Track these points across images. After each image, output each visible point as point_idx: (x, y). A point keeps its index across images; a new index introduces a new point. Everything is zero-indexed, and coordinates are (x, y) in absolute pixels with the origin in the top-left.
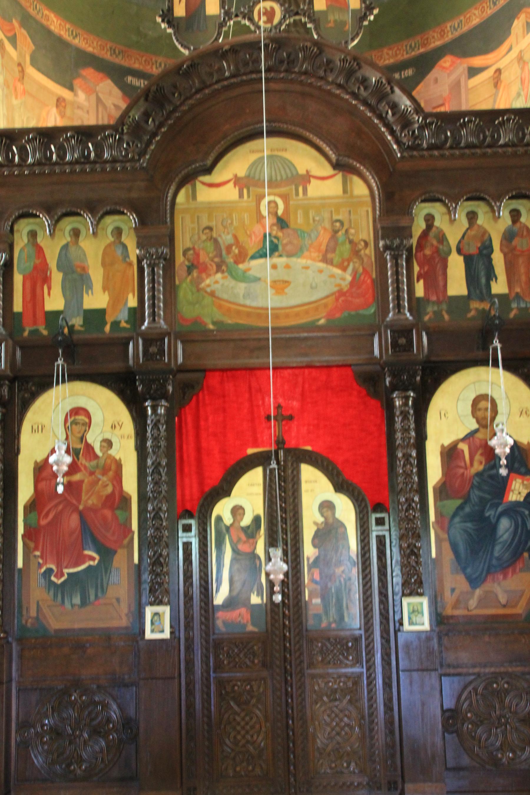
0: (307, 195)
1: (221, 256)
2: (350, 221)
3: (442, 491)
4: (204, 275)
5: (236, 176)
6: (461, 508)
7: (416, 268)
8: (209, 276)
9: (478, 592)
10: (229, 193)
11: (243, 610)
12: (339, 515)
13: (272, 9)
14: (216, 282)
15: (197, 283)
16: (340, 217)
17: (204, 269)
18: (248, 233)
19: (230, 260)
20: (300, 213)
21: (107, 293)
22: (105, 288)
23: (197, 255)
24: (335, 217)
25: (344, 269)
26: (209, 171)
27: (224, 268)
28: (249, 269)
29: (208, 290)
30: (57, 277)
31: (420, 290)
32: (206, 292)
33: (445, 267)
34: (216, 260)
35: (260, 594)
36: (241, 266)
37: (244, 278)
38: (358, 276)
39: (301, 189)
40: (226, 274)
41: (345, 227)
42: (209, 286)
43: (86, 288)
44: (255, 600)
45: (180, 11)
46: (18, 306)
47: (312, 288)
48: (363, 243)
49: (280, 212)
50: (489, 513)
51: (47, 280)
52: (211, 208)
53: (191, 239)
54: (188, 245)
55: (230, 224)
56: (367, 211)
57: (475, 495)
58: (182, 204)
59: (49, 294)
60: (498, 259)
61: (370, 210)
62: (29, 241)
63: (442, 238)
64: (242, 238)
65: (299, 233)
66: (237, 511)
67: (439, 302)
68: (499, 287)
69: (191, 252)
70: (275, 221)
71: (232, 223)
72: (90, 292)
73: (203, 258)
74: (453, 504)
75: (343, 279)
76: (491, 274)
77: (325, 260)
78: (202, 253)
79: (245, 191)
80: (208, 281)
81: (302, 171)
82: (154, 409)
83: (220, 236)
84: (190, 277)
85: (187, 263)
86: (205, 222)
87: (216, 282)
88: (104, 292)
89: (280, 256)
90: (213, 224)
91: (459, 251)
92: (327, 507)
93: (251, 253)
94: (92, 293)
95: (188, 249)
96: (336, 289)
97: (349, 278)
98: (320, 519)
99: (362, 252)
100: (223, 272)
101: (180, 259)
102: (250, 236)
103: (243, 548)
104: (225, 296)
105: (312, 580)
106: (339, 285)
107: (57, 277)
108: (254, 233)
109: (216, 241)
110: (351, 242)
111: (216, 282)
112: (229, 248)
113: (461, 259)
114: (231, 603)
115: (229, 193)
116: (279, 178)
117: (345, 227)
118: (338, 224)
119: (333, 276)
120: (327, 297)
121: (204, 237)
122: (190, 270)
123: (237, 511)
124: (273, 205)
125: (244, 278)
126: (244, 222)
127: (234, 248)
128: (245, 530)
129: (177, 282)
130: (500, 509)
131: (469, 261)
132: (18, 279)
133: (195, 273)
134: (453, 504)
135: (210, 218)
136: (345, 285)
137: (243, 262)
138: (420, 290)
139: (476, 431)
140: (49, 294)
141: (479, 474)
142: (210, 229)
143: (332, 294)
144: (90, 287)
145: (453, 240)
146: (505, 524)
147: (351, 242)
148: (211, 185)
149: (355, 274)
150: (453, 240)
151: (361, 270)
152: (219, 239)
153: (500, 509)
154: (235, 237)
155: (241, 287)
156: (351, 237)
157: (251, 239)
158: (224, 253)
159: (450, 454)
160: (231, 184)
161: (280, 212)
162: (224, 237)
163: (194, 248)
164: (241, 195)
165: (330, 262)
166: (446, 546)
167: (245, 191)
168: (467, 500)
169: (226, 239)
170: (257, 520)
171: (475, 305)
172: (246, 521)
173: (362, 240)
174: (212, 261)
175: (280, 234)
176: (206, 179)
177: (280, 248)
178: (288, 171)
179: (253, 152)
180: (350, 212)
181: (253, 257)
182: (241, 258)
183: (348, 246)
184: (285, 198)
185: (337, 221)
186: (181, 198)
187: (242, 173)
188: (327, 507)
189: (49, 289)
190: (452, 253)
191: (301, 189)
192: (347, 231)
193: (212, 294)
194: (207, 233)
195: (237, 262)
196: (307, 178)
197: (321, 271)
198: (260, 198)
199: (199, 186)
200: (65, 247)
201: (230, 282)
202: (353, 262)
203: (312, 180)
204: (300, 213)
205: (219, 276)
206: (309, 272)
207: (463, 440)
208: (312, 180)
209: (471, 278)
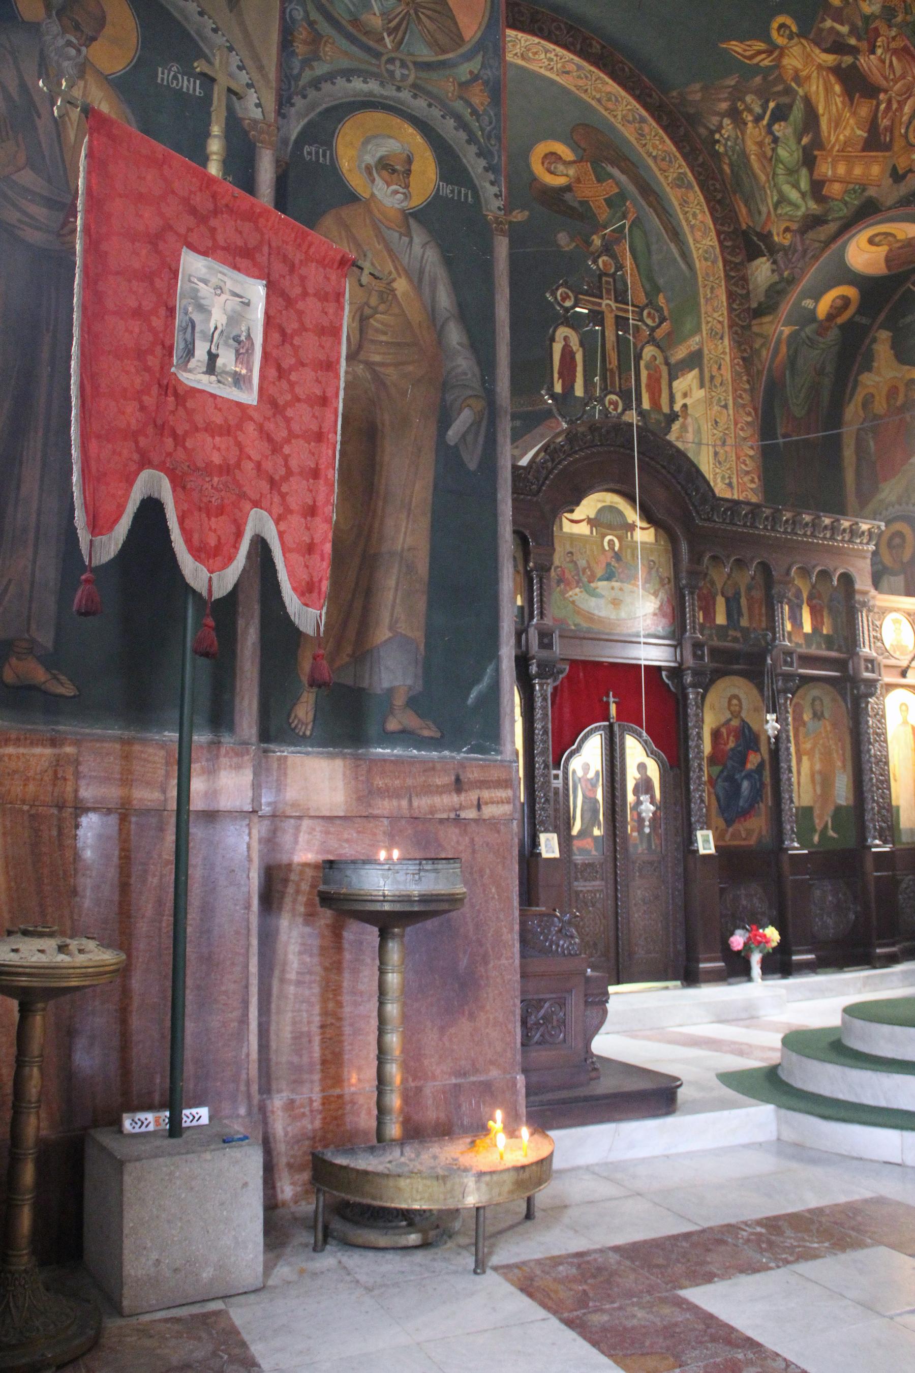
1: (578, 575)
3: (713, 760)
6: (722, 772)
9: (731, 830)
10: (583, 529)
11: (589, 840)
12: (649, 773)
14: (575, 594)
15: (563, 593)
17: (568, 584)
19: (585, 579)
23: (563, 572)
33: (714, 604)
35: (599, 828)
44: (597, 832)
45: (558, 388)
49: (616, 548)
50: (737, 776)
52: (572, 537)
57: (730, 763)
60: (743, 601)
64: (593, 564)
66: (586, 768)
67: (711, 628)
68: (744, 622)
73: (568, 575)
74: (717, 769)
76: (740, 614)
82: (541, 685)
86: (568, 549)
90: (574, 550)
91: (723, 595)
92: (642, 767)
93: (599, 575)
98: (638, 776)
103: (588, 794)
104: (581, 606)
105: (632, 819)
109: (576, 563)
114: (583, 833)
115: (583, 529)
122: (559, 581)
123: (586, 768)
128: (590, 780)
130: (743, 774)
131: (728, 601)
133: (562, 586)
134: (717, 769)
135: (572, 545)
139: (730, 720)
141: (732, 750)
142: (571, 553)
146: (745, 784)
148: (573, 521)
153: (743, 774)
159: (716, 735)
160: (585, 523)
161: (616, 548)
166: (713, 797)
168: (725, 766)
169: (582, 563)
170: (597, 773)
171: (731, 632)
172: (591, 775)
181: (600, 580)
184: (620, 539)
187: (592, 516)
188: (642, 767)
193: (573, 602)
195: (590, 582)
196: (632, 527)
198: (603, 536)
201: (584, 595)
204: (629, 551)
205: (577, 590)
207: (723, 725)
209: (729, 615)
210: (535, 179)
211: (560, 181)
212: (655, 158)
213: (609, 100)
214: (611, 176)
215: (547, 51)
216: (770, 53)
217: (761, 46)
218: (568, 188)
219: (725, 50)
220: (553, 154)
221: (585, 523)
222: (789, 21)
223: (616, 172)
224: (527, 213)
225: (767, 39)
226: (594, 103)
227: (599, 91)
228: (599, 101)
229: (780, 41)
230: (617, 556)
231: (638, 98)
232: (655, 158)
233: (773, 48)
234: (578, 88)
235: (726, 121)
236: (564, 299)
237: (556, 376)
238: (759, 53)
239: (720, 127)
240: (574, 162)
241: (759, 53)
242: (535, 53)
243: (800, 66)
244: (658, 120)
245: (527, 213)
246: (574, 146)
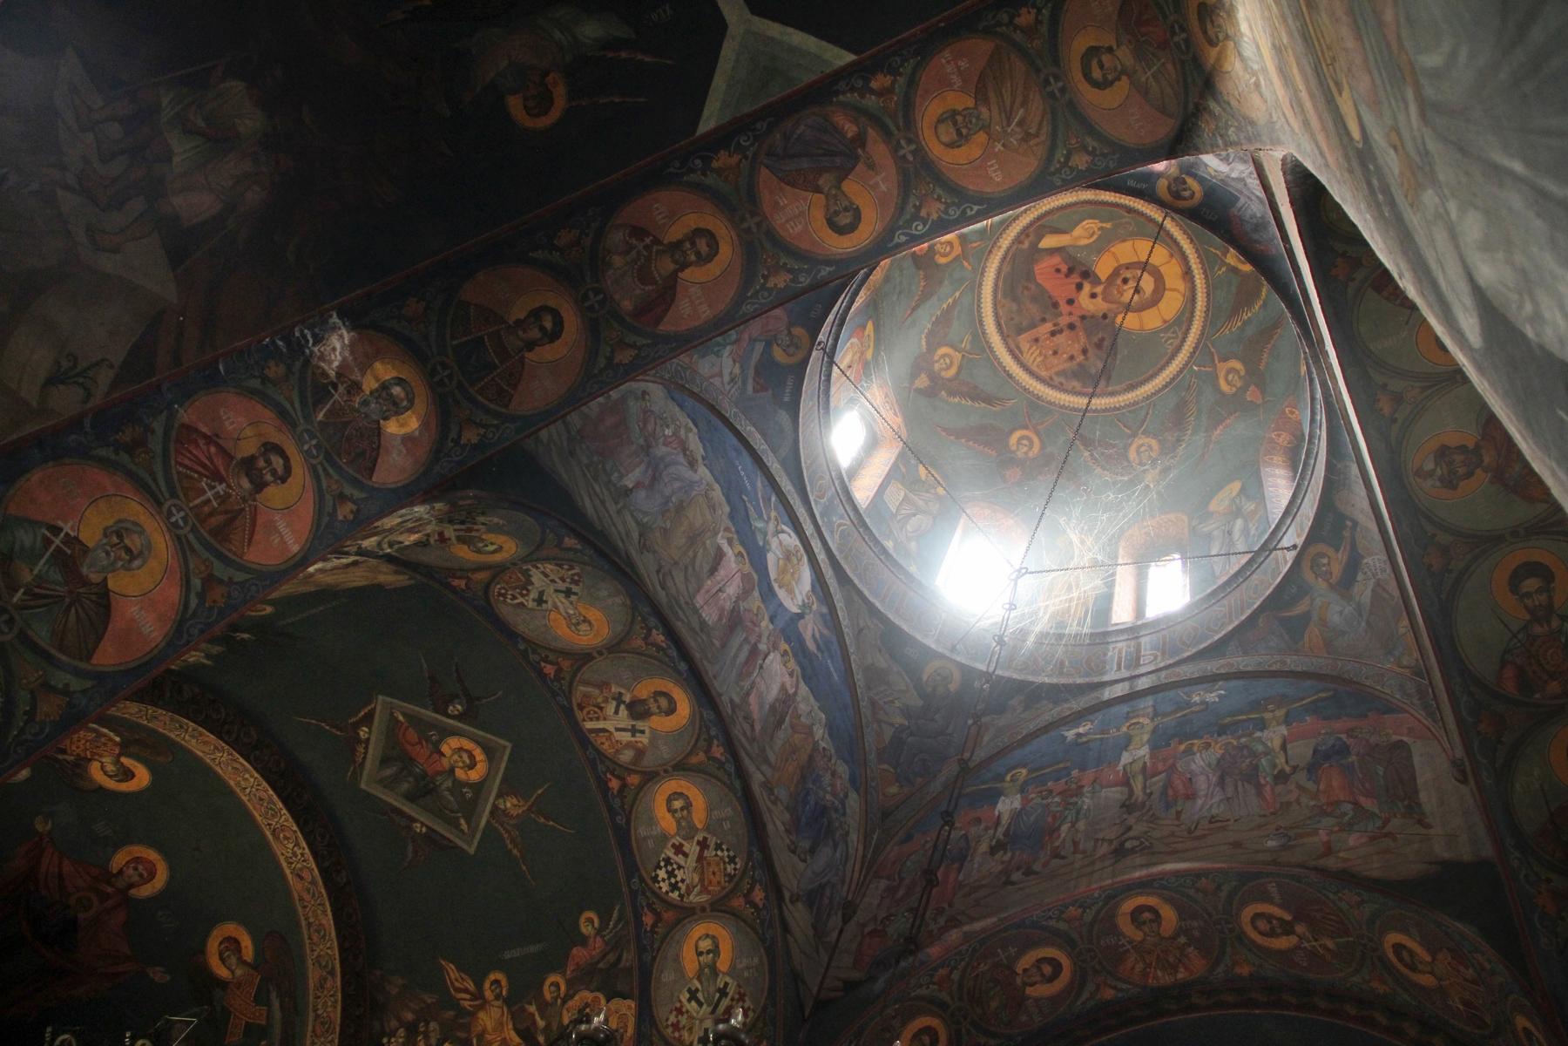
210: (202, 951)
211: (222, 972)
212: (317, 1016)
213: (318, 931)
214: (269, 1004)
215: (297, 845)
216: (475, 997)
217: (471, 986)
218: (223, 985)
219: (441, 968)
220: (236, 941)
222: (504, 982)
223: (276, 1004)
224: (168, 978)
225: (479, 985)
226: (304, 923)
227: (316, 917)
228: (309, 925)
229: (488, 994)
231: (342, 949)
232: (317, 1016)
233: (478, 995)
234: (301, 899)
235: (401, 1032)
238: (466, 991)
239: (393, 1034)
240: (248, 964)
241: (466, 991)
242: (286, 838)
243: (489, 1028)
244: (345, 984)
245: (168, 978)
246: (258, 951)
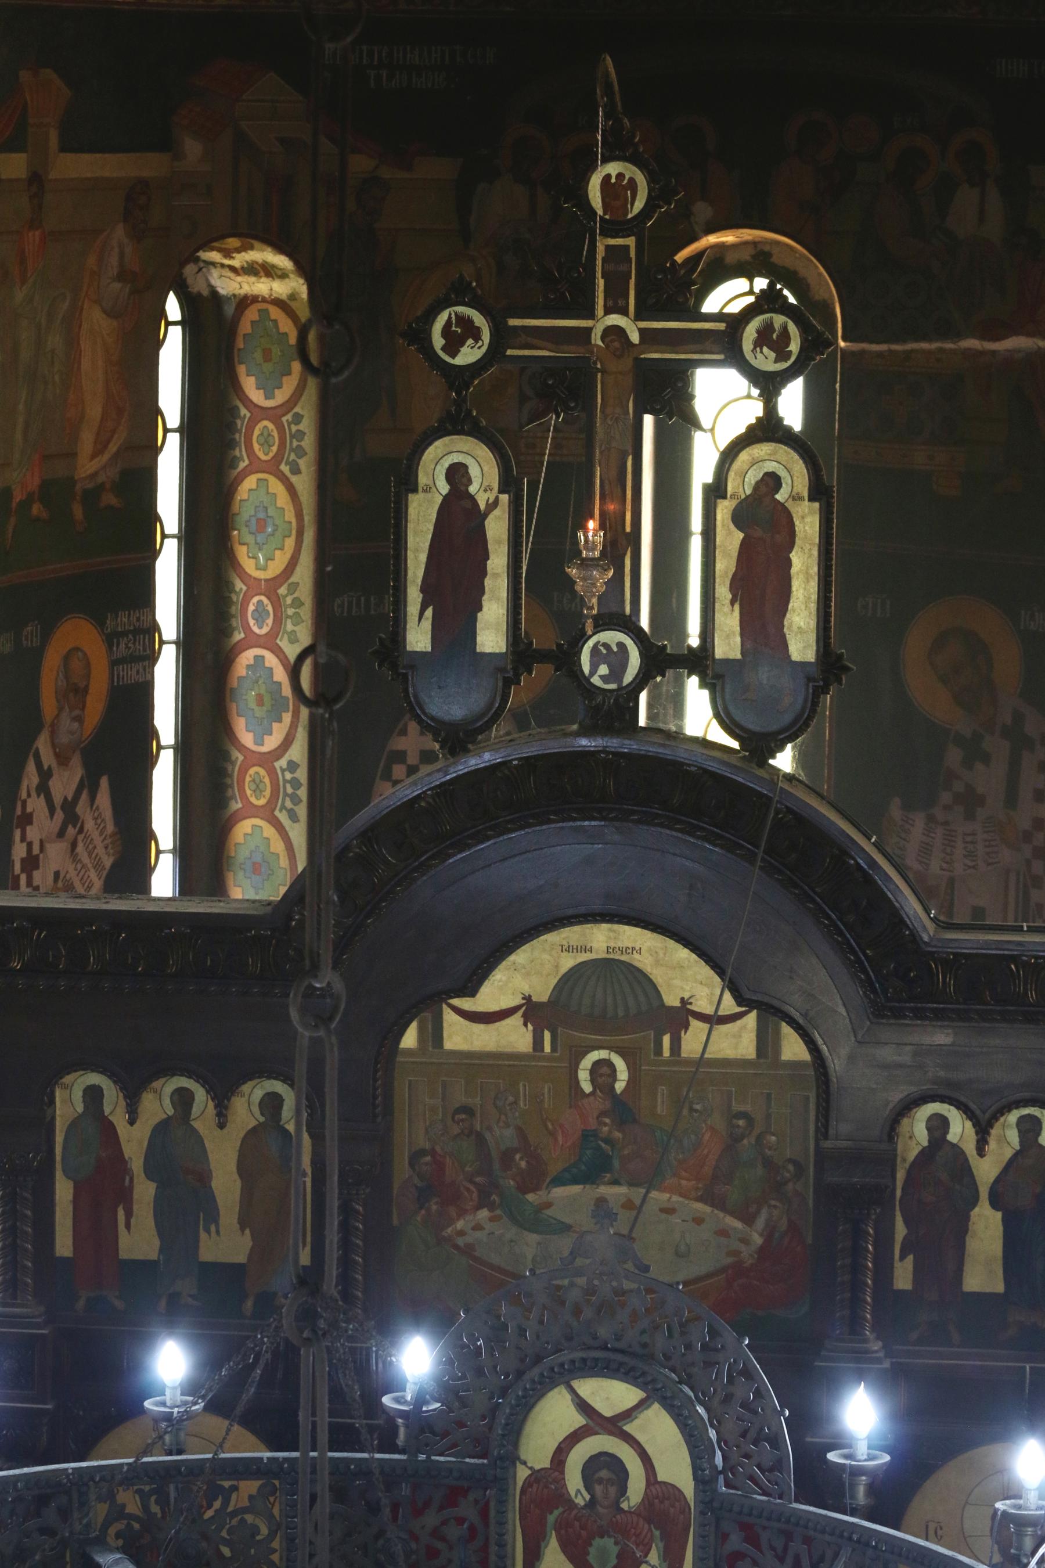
0: (679, 1055)
2: (768, 1116)
4: (452, 1211)
5: (528, 999)
7: (901, 1230)
8: (462, 1213)
10: (515, 1037)
13: (621, 646)
16: (747, 1108)
18: (550, 1126)
20: (662, 1089)
21: (247, 1232)
22: (243, 1223)
24: (737, 1107)
25: (748, 1220)
26: (471, 991)
27: (494, 1197)
28: (549, 1205)
29: (460, 1241)
30: (145, 1191)
31: (903, 1276)
32: (456, 1247)
34: (478, 1179)
36: (530, 1197)
37: (536, 1222)
38: (777, 1235)
39: (666, 1040)
40: (498, 1212)
41: (756, 1132)
42: (461, 1233)
43: (204, 1220)
46: (64, 1245)
47: (677, 1254)
48: (791, 1167)
49: (620, 1086)
51: (125, 1196)
53: (427, 1132)
54: (422, 1143)
55: (511, 1104)
56: (807, 1098)
58: (409, 1052)
59: (128, 1226)
61: (812, 1096)
62: (86, 1107)
63: (963, 1171)
65: (658, 1134)
69: (428, 1158)
70: (608, 1105)
71: (516, 1103)
72: (213, 1228)
75: (745, 1241)
77: (708, 1197)
78: (448, 1160)
79: (547, 1035)
80: (460, 1225)
81: (671, 1000)
83: (489, 1129)
84: (423, 1212)
85: (416, 1180)
86: (460, 1098)
87: (478, 1227)
88: (242, 1229)
89: (615, 1182)
93: (555, 1168)
94: (218, 1232)
95: (422, 1152)
96: (730, 1260)
97: (758, 1240)
99: (790, 1186)
100: (491, 1207)
101: (402, 1170)
102: (553, 1134)
104: (495, 1259)
106: (736, 1253)
107: (145, 1191)
108: (561, 1126)
109: (480, 1141)
110: (768, 1164)
111: (478, 1227)
112: (507, 1158)
113: (996, 1217)
116: (621, 1013)
117: (756, 1132)
118: (741, 1122)
119: (723, 1233)
120: (709, 1276)
121: (456, 1130)
124: (605, 1070)
125: (536, 1222)
126: (542, 1101)
127: (518, 1157)
129: (395, 1222)
132: (64, 1191)
136: (748, 1255)
137: (535, 1189)
138: (903, 1276)
140: (128, 1226)
142: (468, 1110)
143: (723, 1270)
144: (213, 1216)
145: (986, 1170)
147: (768, 1164)
149: (769, 1234)
150: (986, 1170)
151: (783, 1225)
152: (488, 1136)
154: (521, 1132)
155: (530, 1243)
156: (768, 1152)
157: (556, 1140)
158: (497, 1166)
160: (516, 1020)
161: (620, 1086)
162: (497, 1132)
163: (433, 1153)
164: (538, 1043)
165: (719, 1203)
167: (547, 1035)
169: (502, 1136)
173: (790, 1160)
174: (471, 1182)
175: (618, 1135)
176: (465, 1003)
177: (616, 1164)
178: (642, 998)
179: (569, 949)
180: (769, 1095)
181: (559, 1181)
182: (534, 1179)
183: (760, 1171)
185: (744, 1115)
186: (410, 1039)
187: (542, 994)
189: (129, 1214)
190: (980, 1203)
191: (666, 1040)
192: (759, 1138)
193: (468, 1251)
194: (462, 1120)
195: (524, 1189)
196: (681, 1017)
197: (698, 1221)
199: (449, 1017)
200: (162, 1129)
202: (769, 1206)
203: (694, 1023)
204: (662, 1089)
205: (484, 1214)
206: (675, 1219)
208: (694, 1023)
221: (516, 1020)
230: (622, 1109)
236: (453, 345)
237: (414, 596)
